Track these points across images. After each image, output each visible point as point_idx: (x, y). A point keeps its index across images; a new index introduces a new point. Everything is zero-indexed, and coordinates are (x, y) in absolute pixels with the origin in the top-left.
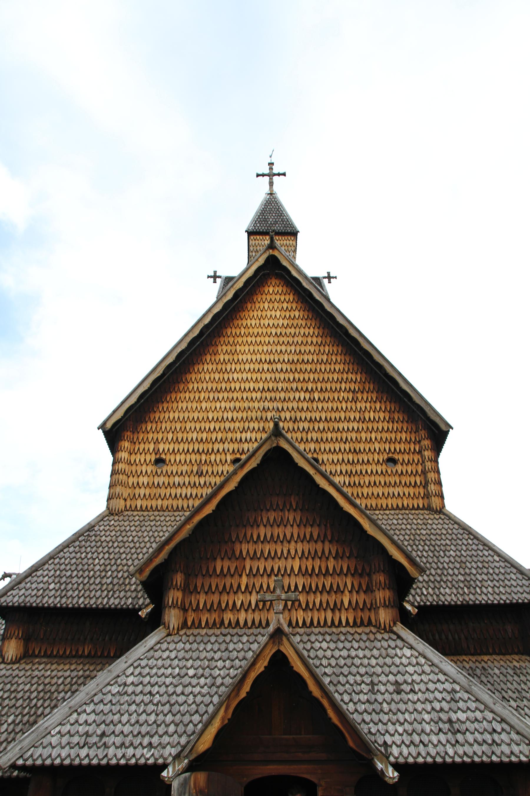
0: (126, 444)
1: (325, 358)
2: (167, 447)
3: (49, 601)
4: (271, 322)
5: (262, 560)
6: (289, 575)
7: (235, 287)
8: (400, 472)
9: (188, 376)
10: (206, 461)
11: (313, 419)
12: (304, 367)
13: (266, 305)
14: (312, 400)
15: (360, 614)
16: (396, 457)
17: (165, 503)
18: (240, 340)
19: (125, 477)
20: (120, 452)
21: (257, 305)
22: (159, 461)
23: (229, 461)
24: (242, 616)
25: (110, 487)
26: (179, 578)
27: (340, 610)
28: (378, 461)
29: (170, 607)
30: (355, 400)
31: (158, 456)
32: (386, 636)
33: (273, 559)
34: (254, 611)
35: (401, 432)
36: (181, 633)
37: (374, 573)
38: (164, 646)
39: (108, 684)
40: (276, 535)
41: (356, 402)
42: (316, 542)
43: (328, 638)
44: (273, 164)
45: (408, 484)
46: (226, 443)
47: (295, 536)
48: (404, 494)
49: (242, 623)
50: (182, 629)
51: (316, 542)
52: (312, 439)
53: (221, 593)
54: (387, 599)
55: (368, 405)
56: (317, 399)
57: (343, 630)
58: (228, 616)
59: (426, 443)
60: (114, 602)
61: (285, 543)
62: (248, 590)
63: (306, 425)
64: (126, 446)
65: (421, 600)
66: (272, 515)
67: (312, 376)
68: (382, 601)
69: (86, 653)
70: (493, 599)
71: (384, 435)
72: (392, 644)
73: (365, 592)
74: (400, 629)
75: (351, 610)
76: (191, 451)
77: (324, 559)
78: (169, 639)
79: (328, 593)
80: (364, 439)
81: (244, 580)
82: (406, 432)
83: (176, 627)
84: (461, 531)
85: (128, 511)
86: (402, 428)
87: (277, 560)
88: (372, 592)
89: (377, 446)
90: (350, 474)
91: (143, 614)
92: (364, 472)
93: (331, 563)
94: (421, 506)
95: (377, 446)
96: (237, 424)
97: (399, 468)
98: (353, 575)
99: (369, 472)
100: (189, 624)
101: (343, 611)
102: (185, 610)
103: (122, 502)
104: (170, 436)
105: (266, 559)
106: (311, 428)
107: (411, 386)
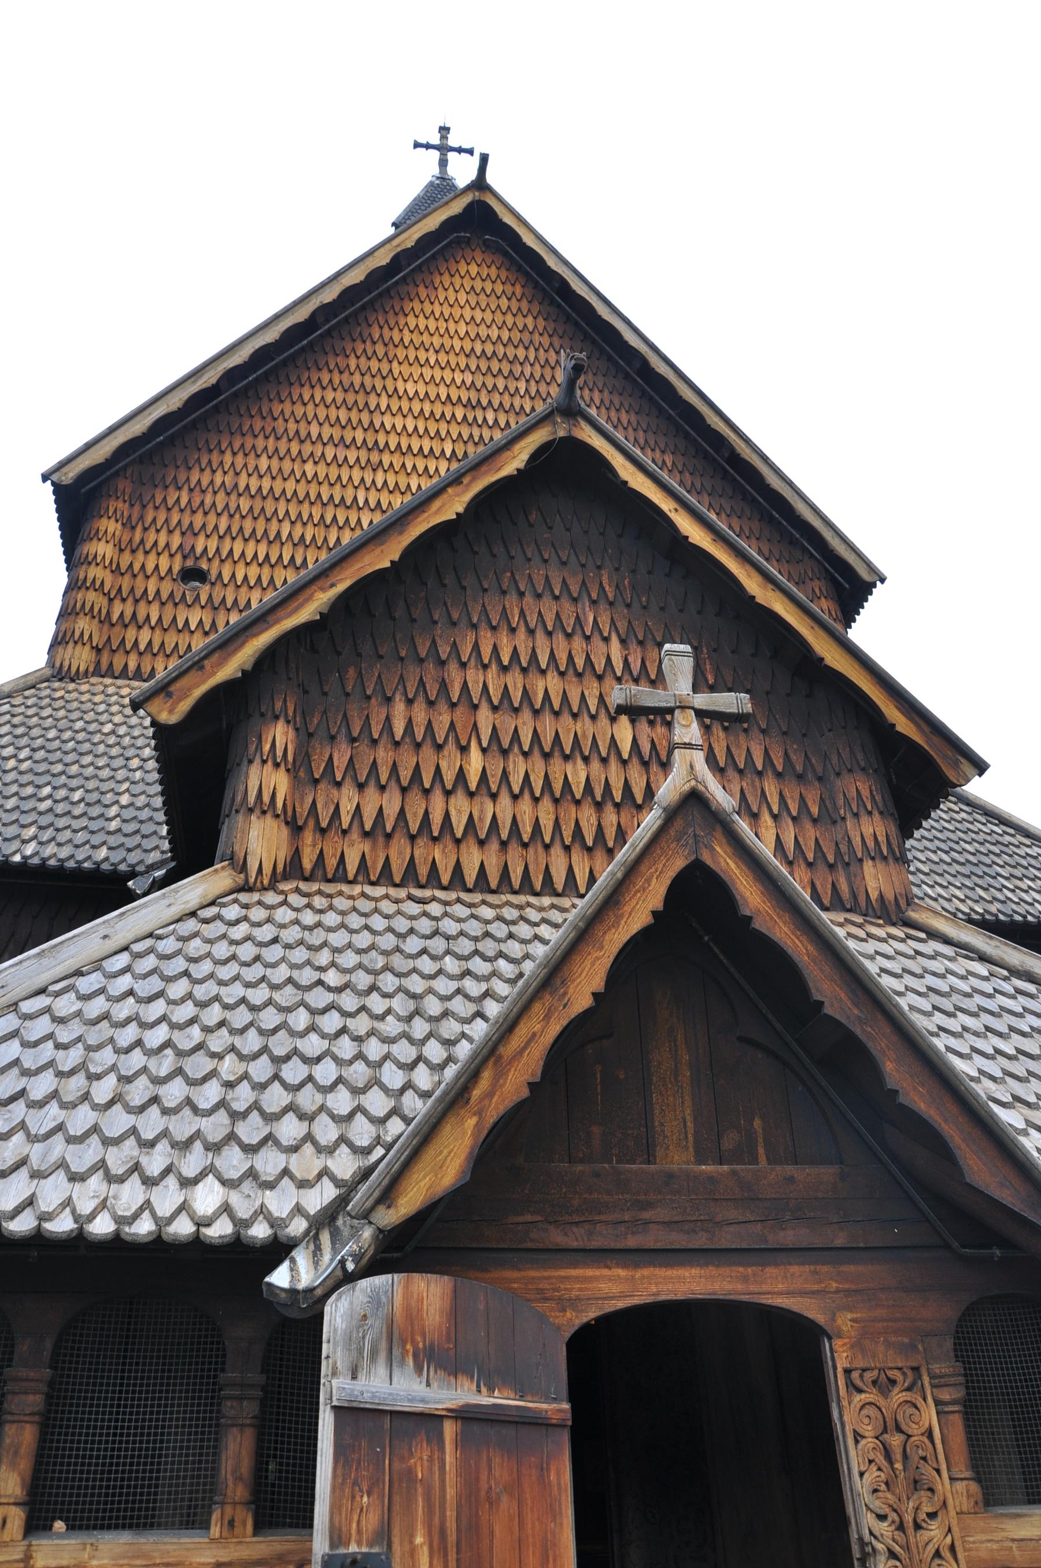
0: (110, 526)
5: (526, 715)
20: (95, 541)
22: (193, 575)
25: (61, 616)
29: (251, 810)
31: (190, 563)
37: (838, 774)
38: (232, 912)
44: (447, 130)
49: (470, 876)
50: (286, 877)
54: (882, 839)
64: (111, 530)
68: (871, 844)
81: (475, 762)
83: (267, 870)
88: (834, 822)
98: (779, 775)
102: (296, 829)
107: (790, 484)
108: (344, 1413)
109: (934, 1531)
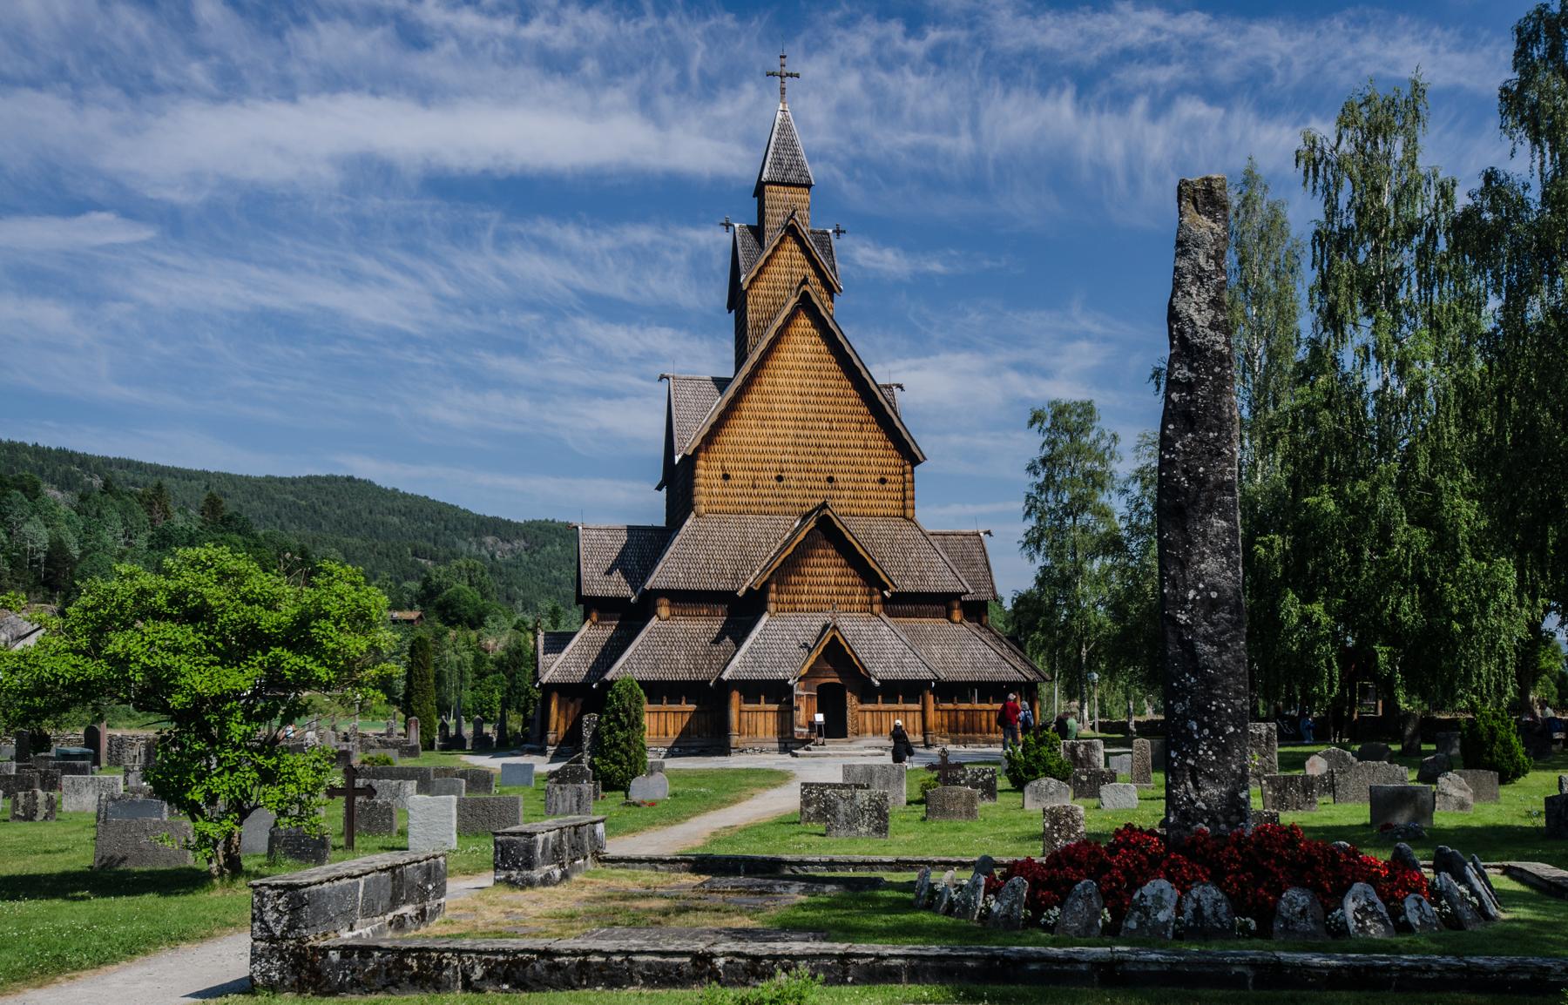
1: (841, 391)
3: (683, 586)
4: (803, 356)
14: (831, 429)
18: (778, 372)
24: (805, 606)
26: (774, 587)
30: (861, 430)
58: (798, 606)
59: (908, 468)
60: (721, 587)
63: (826, 450)
66: (820, 551)
71: (880, 460)
74: (883, 615)
81: (806, 588)
89: (874, 468)
90: (854, 490)
91: (740, 594)
95: (874, 468)
97: (887, 486)
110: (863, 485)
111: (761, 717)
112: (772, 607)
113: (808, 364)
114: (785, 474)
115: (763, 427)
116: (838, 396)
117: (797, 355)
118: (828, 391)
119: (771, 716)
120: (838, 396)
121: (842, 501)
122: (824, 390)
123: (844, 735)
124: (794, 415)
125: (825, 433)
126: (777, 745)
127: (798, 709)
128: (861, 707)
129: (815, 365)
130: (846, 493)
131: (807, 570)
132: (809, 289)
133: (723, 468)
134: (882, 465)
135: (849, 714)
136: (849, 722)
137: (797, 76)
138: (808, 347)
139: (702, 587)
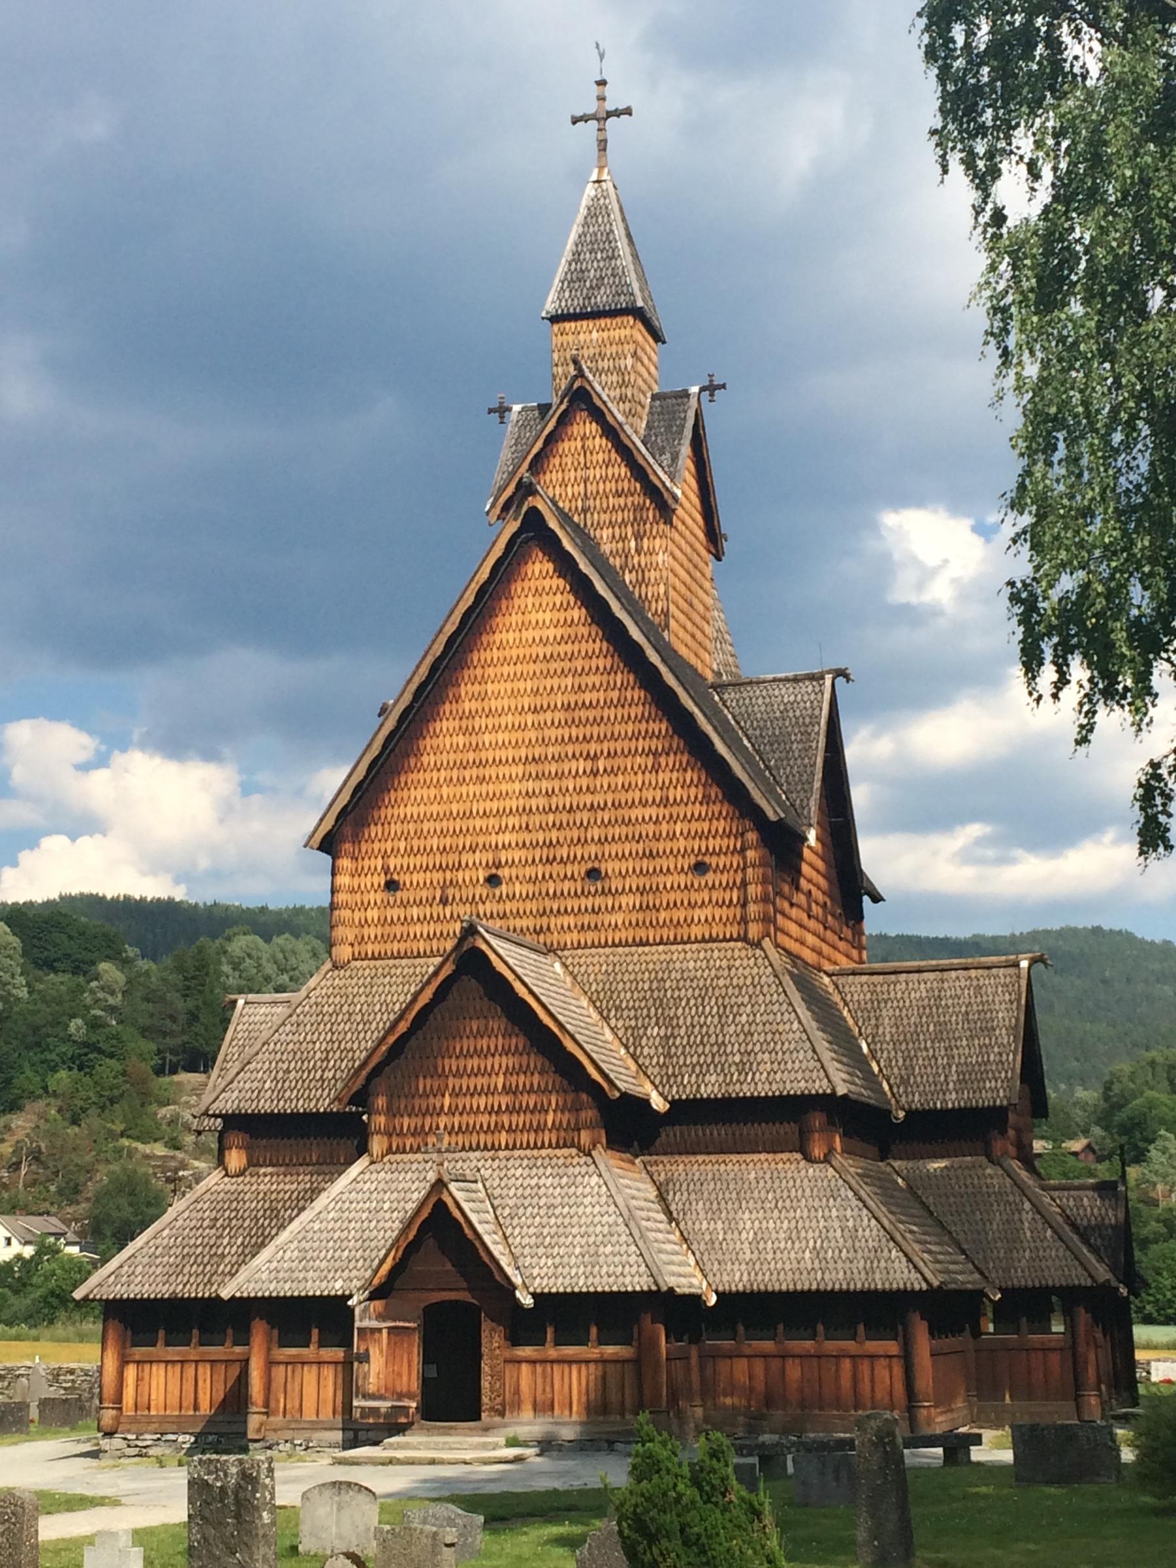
1: (615, 695)
2: (399, 861)
3: (266, 1106)
5: (465, 1077)
6: (493, 1094)
7: (476, 580)
8: (710, 884)
9: (421, 743)
10: (451, 881)
11: (596, 805)
12: (583, 714)
13: (530, 600)
14: (594, 773)
15: (562, 1134)
16: (707, 859)
17: (403, 947)
18: (491, 671)
19: (349, 912)
21: (516, 601)
23: (481, 880)
26: (381, 1102)
27: (543, 1131)
28: (682, 868)
30: (656, 769)
31: (389, 877)
32: (583, 1159)
33: (476, 1075)
34: (457, 1133)
35: (718, 819)
36: (386, 1159)
38: (367, 1176)
39: (311, 1221)
40: (479, 1048)
41: (657, 772)
42: (521, 1054)
43: (525, 1162)
45: (720, 902)
46: (478, 852)
47: (500, 1048)
48: (714, 919)
51: (521, 1054)
52: (593, 839)
53: (424, 1115)
55: (675, 775)
56: (601, 771)
57: (544, 1152)
61: (489, 1056)
62: (452, 1112)
65: (677, 1092)
67: (595, 730)
69: (314, 1160)
70: (763, 1090)
71: (695, 826)
72: (584, 1170)
73: (569, 1111)
75: (554, 1131)
76: (431, 867)
77: (529, 1074)
78: (372, 1167)
79: (532, 1112)
80: (664, 834)
81: (447, 1101)
82: (725, 819)
84: (772, 978)
85: (356, 960)
86: (720, 813)
87: (480, 1077)
89: (682, 843)
90: (642, 891)
92: (661, 887)
93: (536, 1079)
94: (735, 936)
96: (492, 821)
97: (710, 877)
99: (668, 886)
100: (394, 1148)
101: (547, 1132)
102: (390, 1135)
103: (350, 949)
104: (402, 845)
105: (469, 1076)
106: (592, 821)
108: (361, 1330)
109: (498, 1352)
110: (661, 879)
111: (309, 1375)
112: (377, 1144)
113: (548, 650)
114: (504, 873)
115: (462, 781)
116: (609, 704)
117: (528, 635)
118: (588, 697)
119: (329, 1373)
120: (609, 704)
121: (618, 918)
122: (580, 698)
123: (478, 1418)
124: (523, 752)
125: (584, 782)
126: (338, 1436)
127: (365, 1358)
128: (507, 1354)
129: (562, 649)
130: (624, 900)
131: (451, 1064)
132: (539, 507)
133: (386, 871)
134: (701, 836)
135: (485, 1368)
136: (485, 1384)
137: (628, 111)
138: (548, 616)
139: (301, 1106)
